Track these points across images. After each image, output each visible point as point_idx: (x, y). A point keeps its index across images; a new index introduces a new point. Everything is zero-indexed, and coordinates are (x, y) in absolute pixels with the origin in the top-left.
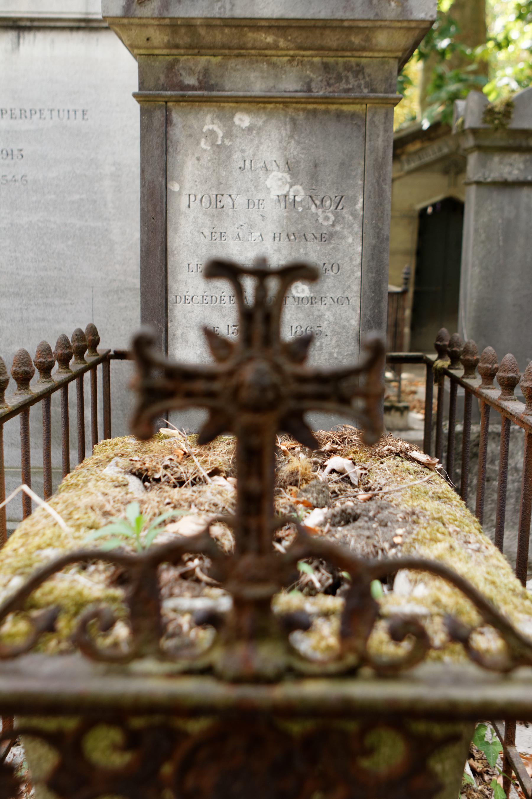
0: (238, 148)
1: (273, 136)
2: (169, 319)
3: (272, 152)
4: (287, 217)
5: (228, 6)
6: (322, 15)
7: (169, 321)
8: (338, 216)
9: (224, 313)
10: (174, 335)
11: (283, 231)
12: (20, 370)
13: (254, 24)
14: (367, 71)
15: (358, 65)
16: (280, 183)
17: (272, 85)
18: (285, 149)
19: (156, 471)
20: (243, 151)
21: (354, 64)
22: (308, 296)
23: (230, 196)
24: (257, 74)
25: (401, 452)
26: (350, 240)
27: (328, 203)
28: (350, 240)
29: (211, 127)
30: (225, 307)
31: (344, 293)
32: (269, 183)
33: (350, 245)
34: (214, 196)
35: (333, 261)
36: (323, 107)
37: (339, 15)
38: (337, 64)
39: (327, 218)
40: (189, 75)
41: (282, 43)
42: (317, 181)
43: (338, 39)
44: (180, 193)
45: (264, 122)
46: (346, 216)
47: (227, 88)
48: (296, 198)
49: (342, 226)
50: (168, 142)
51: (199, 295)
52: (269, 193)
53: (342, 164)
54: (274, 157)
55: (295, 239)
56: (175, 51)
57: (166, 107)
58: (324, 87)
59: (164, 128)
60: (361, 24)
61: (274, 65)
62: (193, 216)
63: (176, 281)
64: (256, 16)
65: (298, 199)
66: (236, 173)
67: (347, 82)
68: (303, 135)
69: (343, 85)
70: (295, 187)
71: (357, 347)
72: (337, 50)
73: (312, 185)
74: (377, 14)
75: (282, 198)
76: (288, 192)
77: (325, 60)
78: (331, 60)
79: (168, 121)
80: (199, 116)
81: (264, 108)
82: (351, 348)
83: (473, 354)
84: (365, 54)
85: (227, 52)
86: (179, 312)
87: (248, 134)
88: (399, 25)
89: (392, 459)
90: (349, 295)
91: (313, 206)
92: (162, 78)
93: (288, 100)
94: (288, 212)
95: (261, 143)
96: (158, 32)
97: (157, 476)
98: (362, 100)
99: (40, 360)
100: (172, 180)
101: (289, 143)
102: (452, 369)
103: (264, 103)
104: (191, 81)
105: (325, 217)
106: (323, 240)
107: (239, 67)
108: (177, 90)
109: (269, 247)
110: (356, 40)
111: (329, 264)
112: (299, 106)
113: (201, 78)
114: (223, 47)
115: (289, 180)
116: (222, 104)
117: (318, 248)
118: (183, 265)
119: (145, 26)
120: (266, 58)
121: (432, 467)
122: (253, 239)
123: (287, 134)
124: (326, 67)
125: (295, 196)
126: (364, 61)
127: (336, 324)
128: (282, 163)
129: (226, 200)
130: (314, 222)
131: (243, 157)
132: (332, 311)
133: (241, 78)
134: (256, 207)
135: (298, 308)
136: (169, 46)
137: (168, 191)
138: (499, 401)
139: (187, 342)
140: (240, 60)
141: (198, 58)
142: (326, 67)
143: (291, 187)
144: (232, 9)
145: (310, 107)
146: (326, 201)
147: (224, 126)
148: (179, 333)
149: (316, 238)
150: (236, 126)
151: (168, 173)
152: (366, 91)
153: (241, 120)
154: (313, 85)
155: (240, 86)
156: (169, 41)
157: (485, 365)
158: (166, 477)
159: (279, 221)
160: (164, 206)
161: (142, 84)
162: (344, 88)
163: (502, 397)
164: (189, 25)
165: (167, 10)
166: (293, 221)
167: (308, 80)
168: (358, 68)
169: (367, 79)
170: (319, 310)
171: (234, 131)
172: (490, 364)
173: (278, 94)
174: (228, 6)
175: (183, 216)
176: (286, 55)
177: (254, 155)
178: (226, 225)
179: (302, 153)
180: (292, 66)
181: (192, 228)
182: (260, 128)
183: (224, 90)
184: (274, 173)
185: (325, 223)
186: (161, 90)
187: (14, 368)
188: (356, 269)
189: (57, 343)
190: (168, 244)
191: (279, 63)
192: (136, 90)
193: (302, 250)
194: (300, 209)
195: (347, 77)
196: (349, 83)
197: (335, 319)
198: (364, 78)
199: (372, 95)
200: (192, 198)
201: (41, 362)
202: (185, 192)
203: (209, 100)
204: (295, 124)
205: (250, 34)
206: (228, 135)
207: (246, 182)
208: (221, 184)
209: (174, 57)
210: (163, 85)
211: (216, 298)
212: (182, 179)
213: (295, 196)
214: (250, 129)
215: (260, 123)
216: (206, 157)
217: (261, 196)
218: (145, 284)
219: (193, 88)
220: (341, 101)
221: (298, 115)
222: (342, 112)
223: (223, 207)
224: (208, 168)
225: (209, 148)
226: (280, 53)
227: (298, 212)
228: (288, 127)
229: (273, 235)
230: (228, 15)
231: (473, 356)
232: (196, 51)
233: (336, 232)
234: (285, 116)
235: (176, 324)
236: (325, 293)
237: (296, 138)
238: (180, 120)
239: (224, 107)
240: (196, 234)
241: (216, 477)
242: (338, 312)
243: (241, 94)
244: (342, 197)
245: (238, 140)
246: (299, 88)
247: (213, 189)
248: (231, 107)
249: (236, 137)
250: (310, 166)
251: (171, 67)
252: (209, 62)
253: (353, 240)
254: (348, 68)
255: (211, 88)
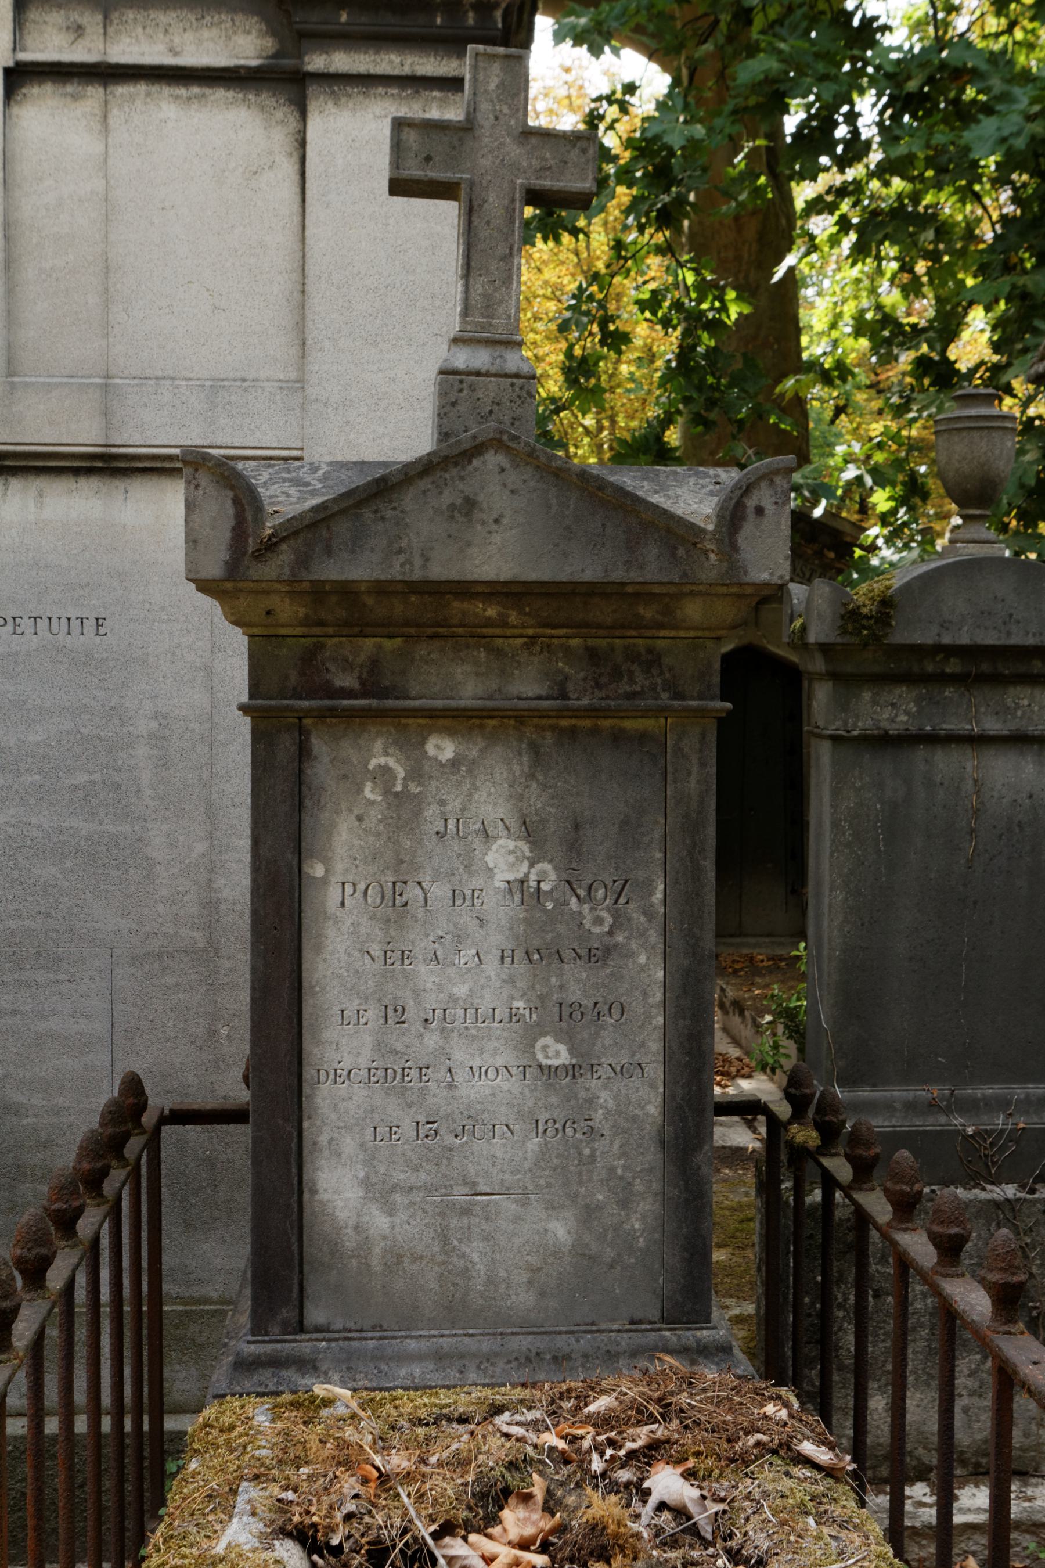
0: (434, 797)
1: (497, 776)
2: (305, 1115)
3: (495, 804)
4: (525, 918)
5: (418, 562)
6: (588, 576)
7: (305, 1117)
8: (620, 916)
9: (409, 1100)
10: (315, 1144)
11: (519, 945)
12: (31, 1256)
13: (465, 590)
14: (667, 661)
15: (650, 651)
16: (511, 859)
17: (494, 686)
18: (521, 797)
19: (332, 1529)
20: (442, 803)
21: (643, 651)
22: (567, 1063)
23: (419, 883)
24: (467, 668)
25: (781, 1445)
26: (642, 959)
27: (601, 893)
28: (642, 959)
29: (382, 760)
30: (412, 1088)
31: (633, 1055)
32: (490, 859)
33: (642, 969)
34: (390, 884)
35: (611, 998)
36: (587, 723)
37: (618, 575)
38: (613, 649)
39: (599, 921)
40: (344, 670)
41: (513, 617)
42: (579, 854)
43: (615, 611)
44: (325, 881)
45: (481, 750)
46: (635, 915)
47: (413, 694)
48: (542, 885)
49: (627, 934)
50: (304, 789)
51: (362, 1066)
52: (492, 878)
53: (625, 823)
54: (501, 812)
55: (542, 959)
56: (317, 630)
57: (300, 727)
58: (590, 690)
59: (296, 764)
60: (657, 590)
61: (499, 653)
62: (350, 921)
63: (319, 1043)
64: (469, 578)
65: (545, 887)
66: (431, 843)
67: (632, 681)
68: (552, 773)
69: (625, 687)
70: (539, 866)
71: (660, 1156)
72: (612, 627)
73: (570, 862)
74: (685, 574)
75: (515, 886)
76: (527, 875)
77: (590, 642)
78: (603, 643)
79: (303, 752)
80: (361, 742)
81: (481, 727)
82: (649, 1157)
83: (868, 1145)
84: (662, 633)
85: (412, 631)
86: (324, 1099)
87: (452, 773)
88: (724, 590)
89: (766, 1467)
90: (644, 1060)
91: (574, 900)
92: (293, 678)
93: (526, 713)
94: (526, 911)
95: (477, 789)
96: (287, 601)
97: (335, 1542)
98: (661, 711)
99: (57, 1206)
100: (312, 857)
101: (527, 787)
102: (824, 1155)
103: (481, 717)
104: (346, 680)
105: (596, 920)
106: (593, 959)
107: (433, 656)
108: (321, 699)
109: (493, 974)
110: (648, 612)
111: (605, 1003)
112: (544, 721)
113: (365, 675)
114: (407, 624)
115: (528, 854)
116: (404, 721)
117: (584, 975)
118: (331, 1012)
119: (267, 592)
120: (483, 641)
121: (839, 1475)
122: (462, 961)
123: (523, 771)
124: (593, 655)
125: (539, 882)
126: (659, 643)
127: (620, 1113)
128: (513, 823)
129: (413, 892)
130: (576, 928)
131: (443, 813)
132: (611, 1090)
133: (438, 675)
134: (468, 903)
135: (548, 1086)
136: (306, 622)
137: (304, 876)
138: (935, 1277)
139: (339, 1155)
140: (437, 643)
141: (360, 641)
142: (593, 655)
143: (532, 866)
144: (424, 567)
145: (564, 723)
146: (597, 891)
147: (408, 758)
148: (323, 1139)
149: (580, 957)
150: (429, 758)
151: (303, 844)
152: (665, 696)
153: (437, 747)
154: (570, 686)
155: (436, 689)
156: (307, 616)
157: (898, 1187)
158: (352, 1540)
159: (511, 928)
160: (297, 905)
161: (255, 688)
162: (625, 692)
163: (940, 1269)
164: (346, 591)
165: (307, 568)
166: (536, 927)
167: (560, 678)
168: (650, 657)
169: (667, 675)
170: (587, 1089)
171: (426, 768)
172: (907, 1184)
173: (507, 704)
174: (418, 562)
175: (331, 922)
176: (521, 636)
177: (463, 810)
178: (412, 937)
179: (552, 805)
180: (531, 654)
181: (348, 943)
182: (474, 762)
183: (407, 698)
184: (501, 842)
185: (597, 930)
186: (290, 699)
187: (19, 1252)
188: (654, 1011)
189: (81, 1148)
190: (304, 975)
191: (507, 649)
192: (245, 698)
193: (553, 980)
194: (550, 906)
195: (631, 673)
196: (636, 683)
197: (619, 1105)
198: (662, 673)
199: (676, 703)
200: (349, 889)
201: (59, 1210)
202: (336, 879)
203: (381, 714)
204: (537, 753)
205: (456, 604)
206: (416, 774)
207: (450, 858)
208: (402, 862)
209: (315, 640)
210: (294, 689)
211: (395, 1072)
212: (330, 854)
213: (539, 882)
214: (454, 764)
215: (474, 753)
216: (374, 815)
217: (476, 883)
218: (259, 1051)
219: (350, 694)
220: (622, 714)
221: (544, 738)
222: (622, 730)
223: (406, 904)
224: (378, 835)
225: (380, 798)
226: (509, 632)
227: (545, 911)
228: (525, 758)
229: (499, 953)
230: (417, 575)
231: (869, 1148)
232: (356, 630)
233: (616, 945)
234: (520, 740)
235: (318, 1123)
236: (599, 1058)
237: (541, 778)
238: (325, 749)
239: (406, 726)
240: (356, 954)
241: (447, 1540)
242: (623, 1091)
243: (439, 703)
244: (626, 881)
245: (434, 783)
246: (544, 693)
247: (389, 872)
248: (419, 725)
249: (431, 777)
250: (566, 828)
251: (309, 658)
252: (380, 647)
253: (648, 958)
254: (632, 656)
255: (384, 693)
